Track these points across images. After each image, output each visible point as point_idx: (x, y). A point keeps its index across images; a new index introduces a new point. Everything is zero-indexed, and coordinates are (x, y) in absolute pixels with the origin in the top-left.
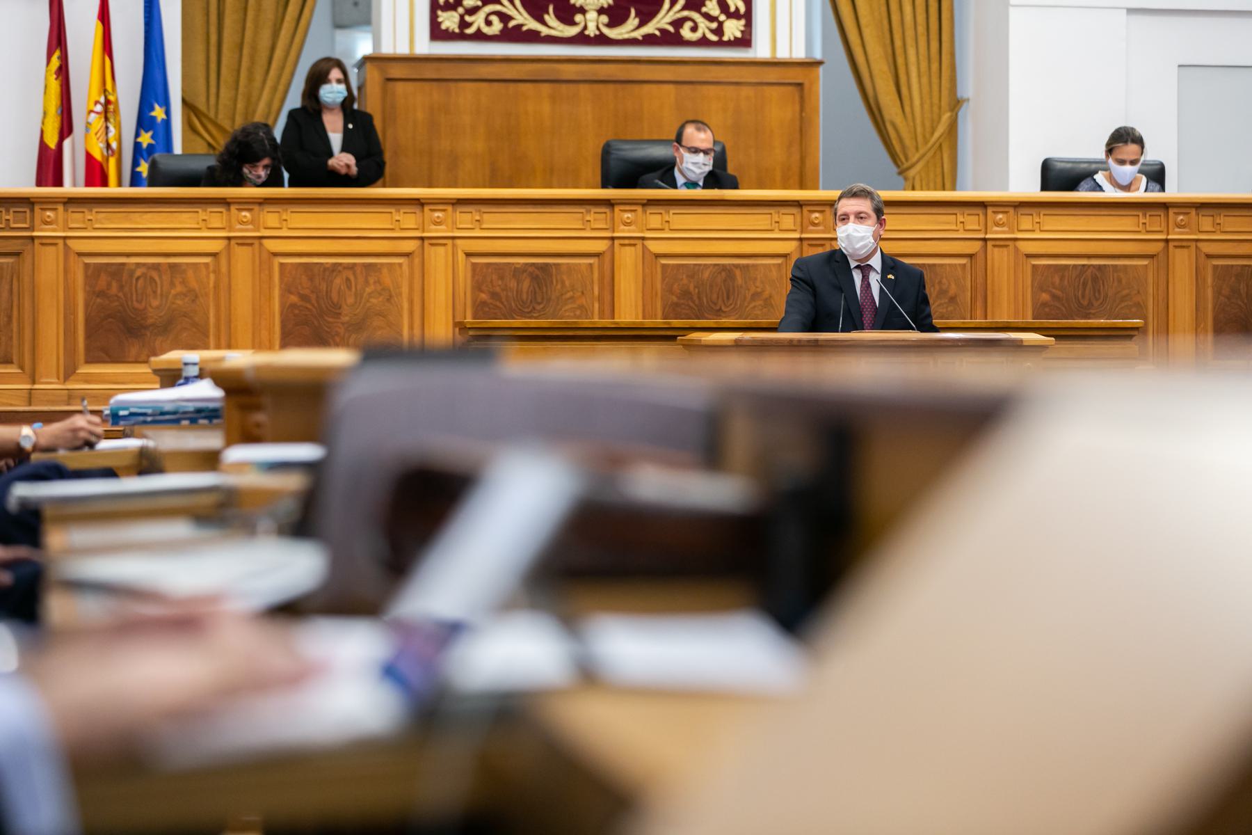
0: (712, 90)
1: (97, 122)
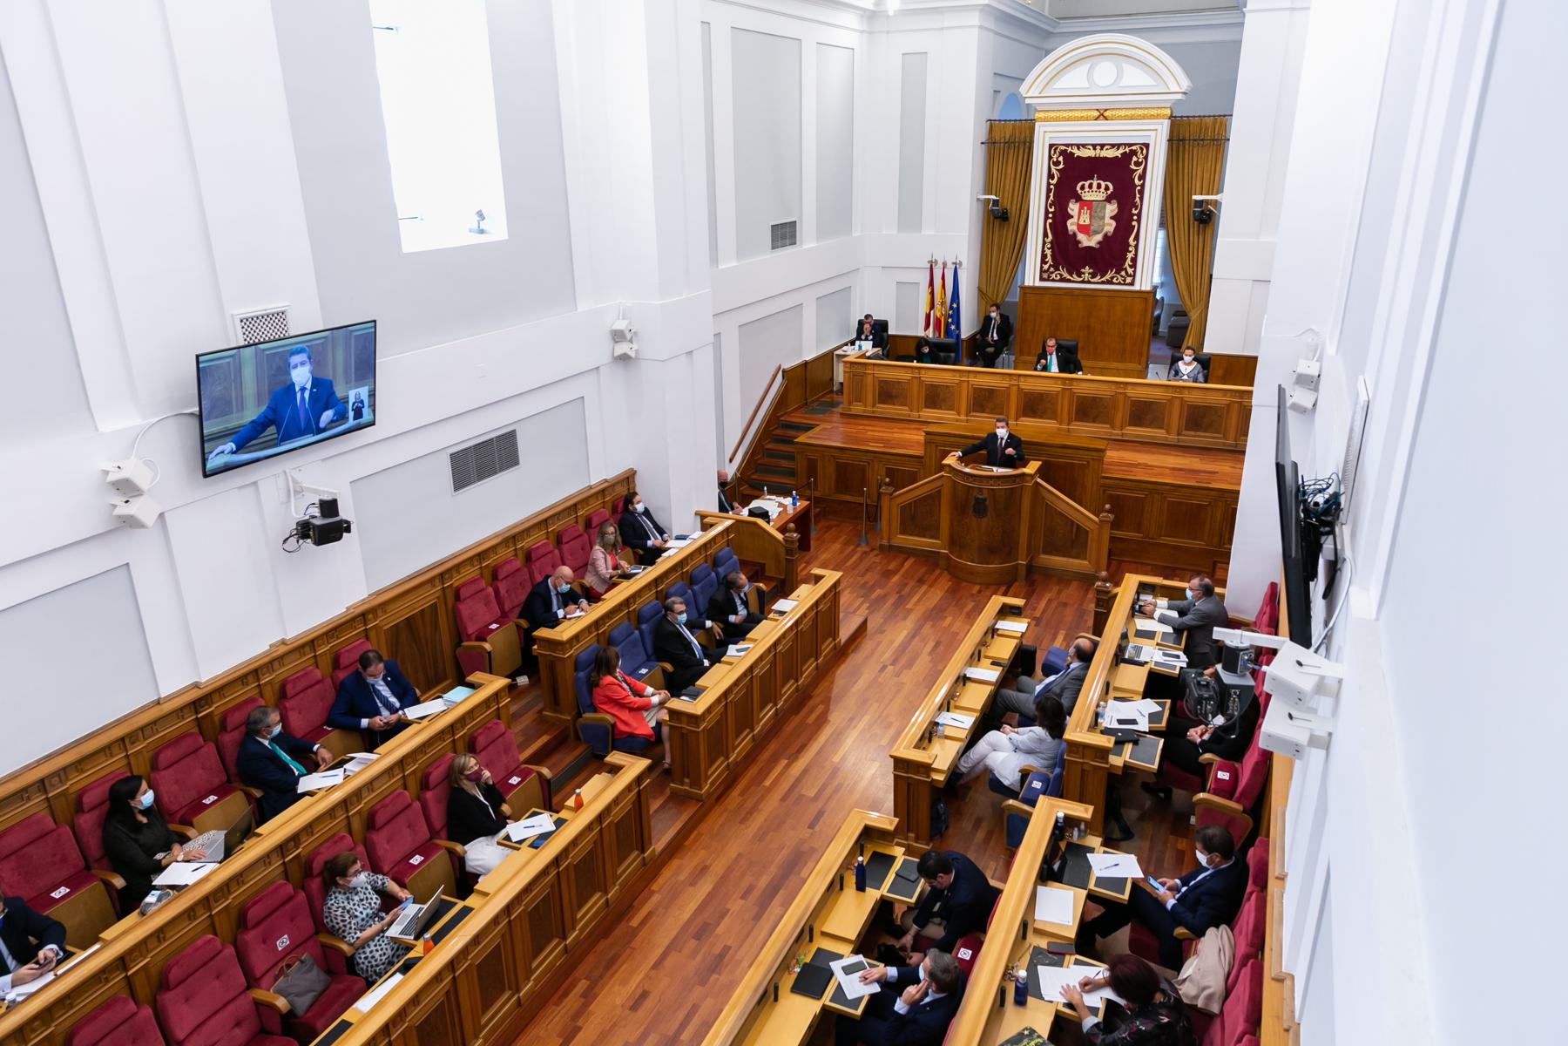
0: (1121, 299)
1: (939, 307)
